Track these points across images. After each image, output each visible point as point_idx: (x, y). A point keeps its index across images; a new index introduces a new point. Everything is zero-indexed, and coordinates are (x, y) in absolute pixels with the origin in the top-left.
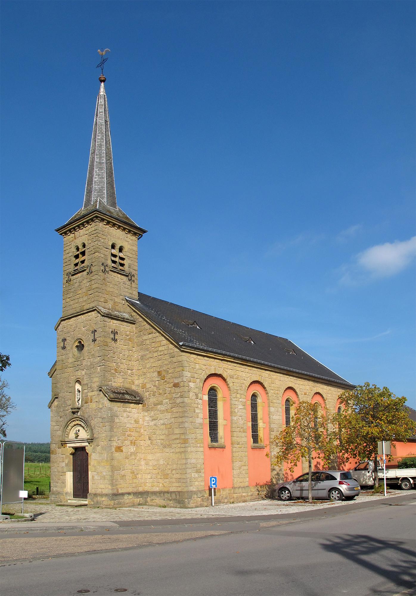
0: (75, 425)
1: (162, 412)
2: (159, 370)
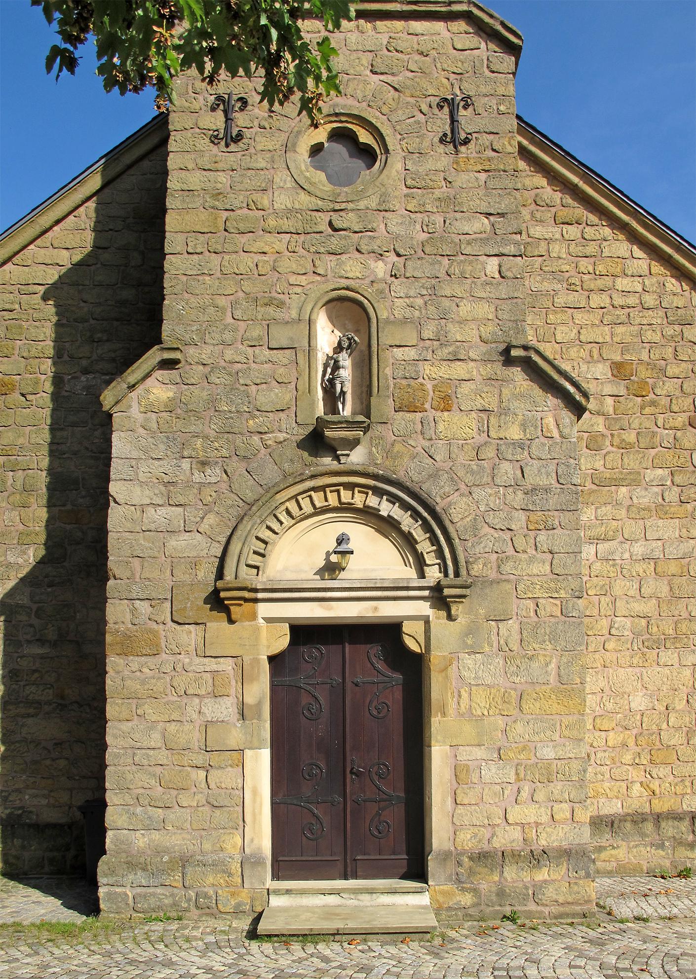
0: (345, 508)
1: (637, 512)
2: (618, 358)
